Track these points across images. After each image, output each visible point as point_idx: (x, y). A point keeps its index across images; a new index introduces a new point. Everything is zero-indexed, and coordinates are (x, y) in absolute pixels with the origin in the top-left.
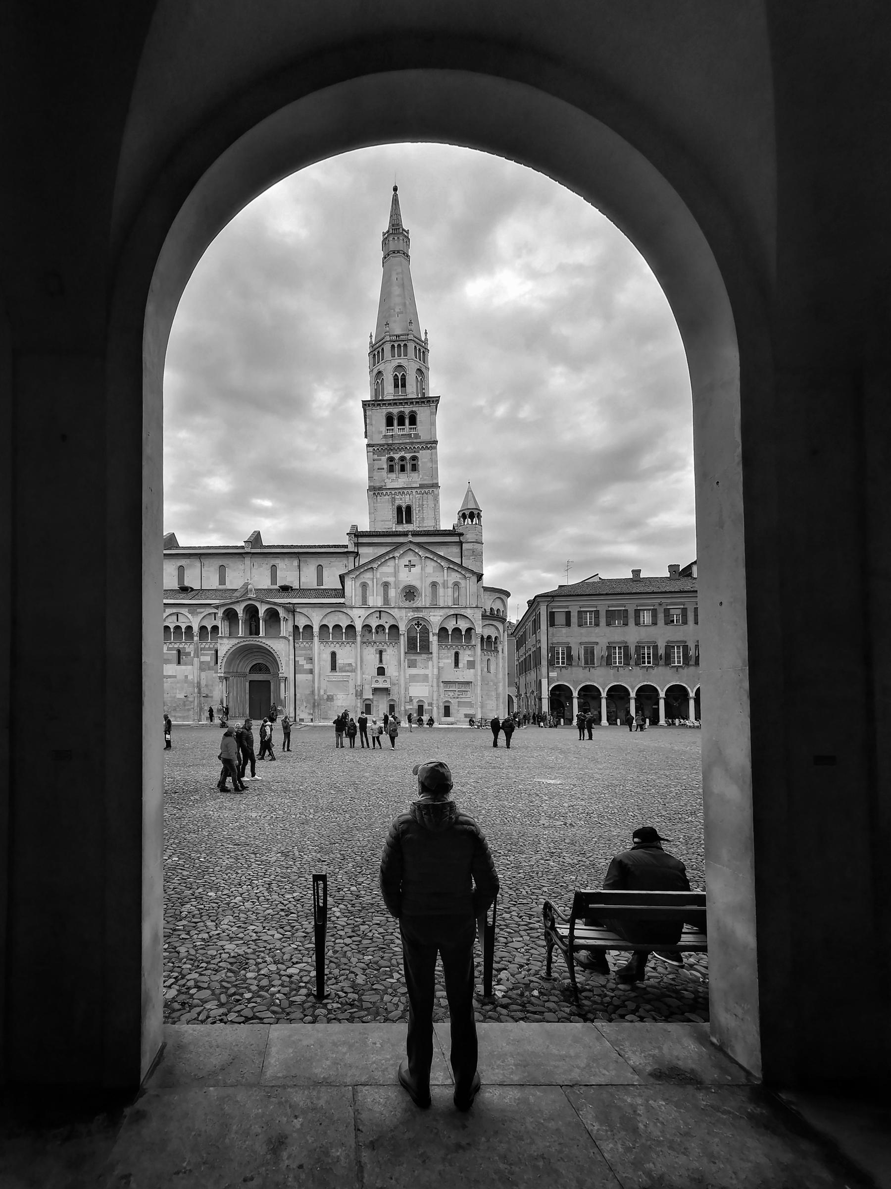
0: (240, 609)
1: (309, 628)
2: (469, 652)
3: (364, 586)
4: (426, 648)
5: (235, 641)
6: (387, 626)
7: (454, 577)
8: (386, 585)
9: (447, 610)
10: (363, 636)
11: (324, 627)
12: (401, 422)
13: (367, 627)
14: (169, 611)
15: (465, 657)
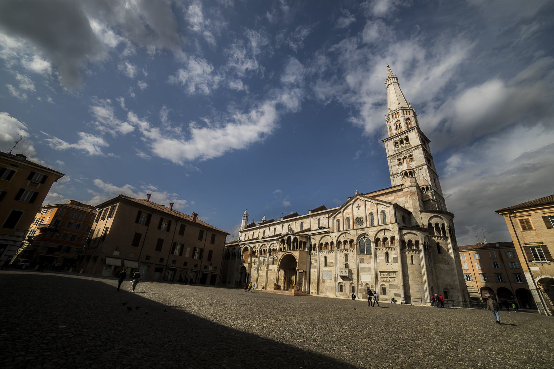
0: (285, 238)
1: (315, 245)
2: (394, 252)
3: (338, 220)
4: (369, 252)
5: (283, 253)
6: (348, 241)
7: (381, 208)
8: (348, 219)
9: (378, 227)
10: (338, 247)
11: (321, 245)
12: (402, 142)
13: (339, 243)
14: (271, 242)
15: (392, 255)
